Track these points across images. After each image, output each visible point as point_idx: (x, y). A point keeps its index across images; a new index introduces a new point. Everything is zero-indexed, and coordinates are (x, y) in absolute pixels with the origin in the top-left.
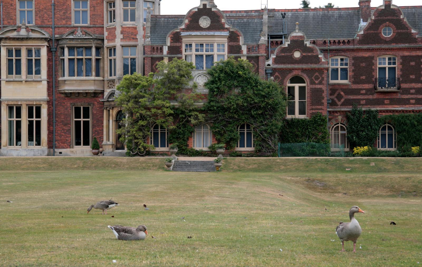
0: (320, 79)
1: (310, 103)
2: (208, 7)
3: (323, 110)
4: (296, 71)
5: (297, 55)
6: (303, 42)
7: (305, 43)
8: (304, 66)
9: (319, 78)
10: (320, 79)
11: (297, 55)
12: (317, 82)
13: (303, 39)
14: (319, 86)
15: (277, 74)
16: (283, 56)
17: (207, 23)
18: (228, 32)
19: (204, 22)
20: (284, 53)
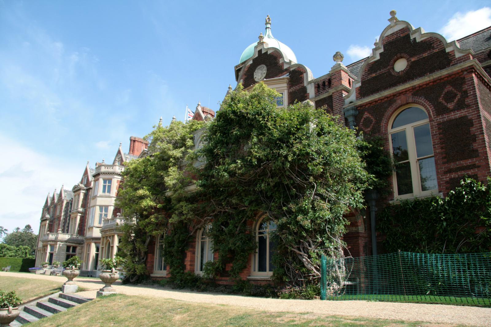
0: (459, 96)
1: (445, 158)
2: (263, 52)
3: (478, 167)
4: (403, 97)
5: (401, 66)
6: (408, 36)
7: (412, 37)
8: (417, 82)
9: (456, 95)
10: (459, 96)
11: (401, 66)
12: (450, 106)
13: (406, 33)
14: (458, 114)
15: (366, 115)
16: (374, 78)
17: (261, 74)
18: (288, 74)
19: (260, 73)
20: (375, 72)
